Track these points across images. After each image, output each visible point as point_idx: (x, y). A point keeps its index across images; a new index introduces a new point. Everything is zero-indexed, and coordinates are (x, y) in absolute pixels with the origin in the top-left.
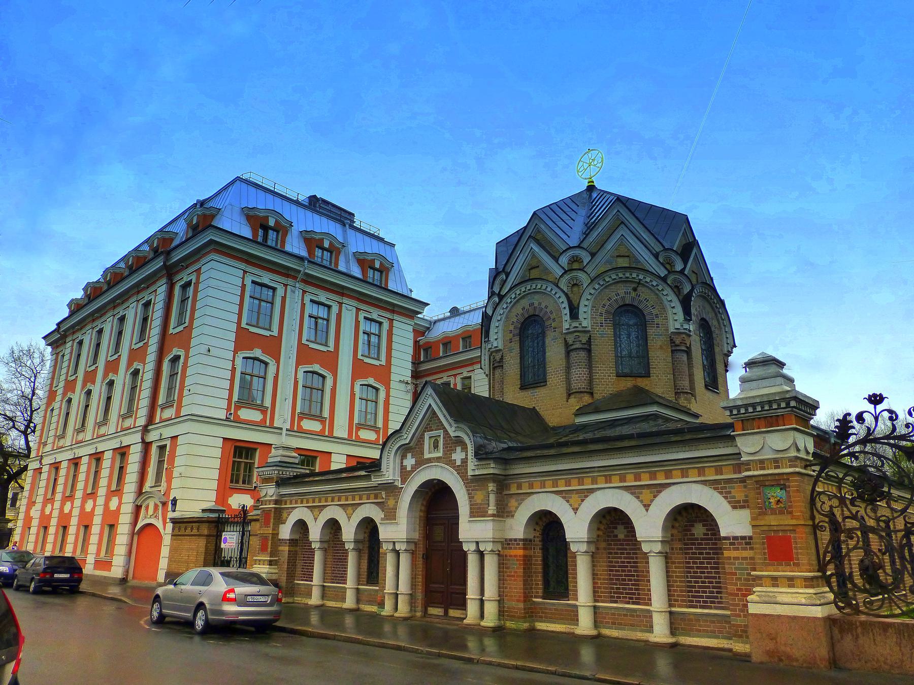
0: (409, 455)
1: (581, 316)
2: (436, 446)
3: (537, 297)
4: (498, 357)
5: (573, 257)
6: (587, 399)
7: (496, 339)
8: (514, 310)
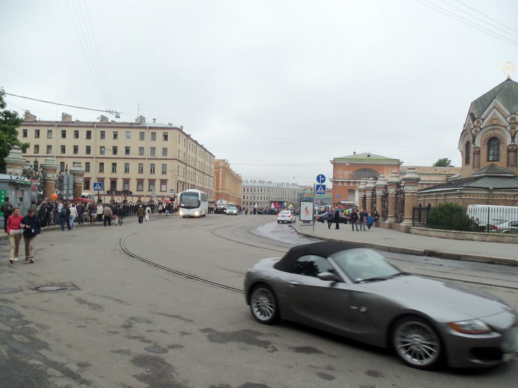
4: (478, 150)
5: (512, 117)
7: (478, 144)
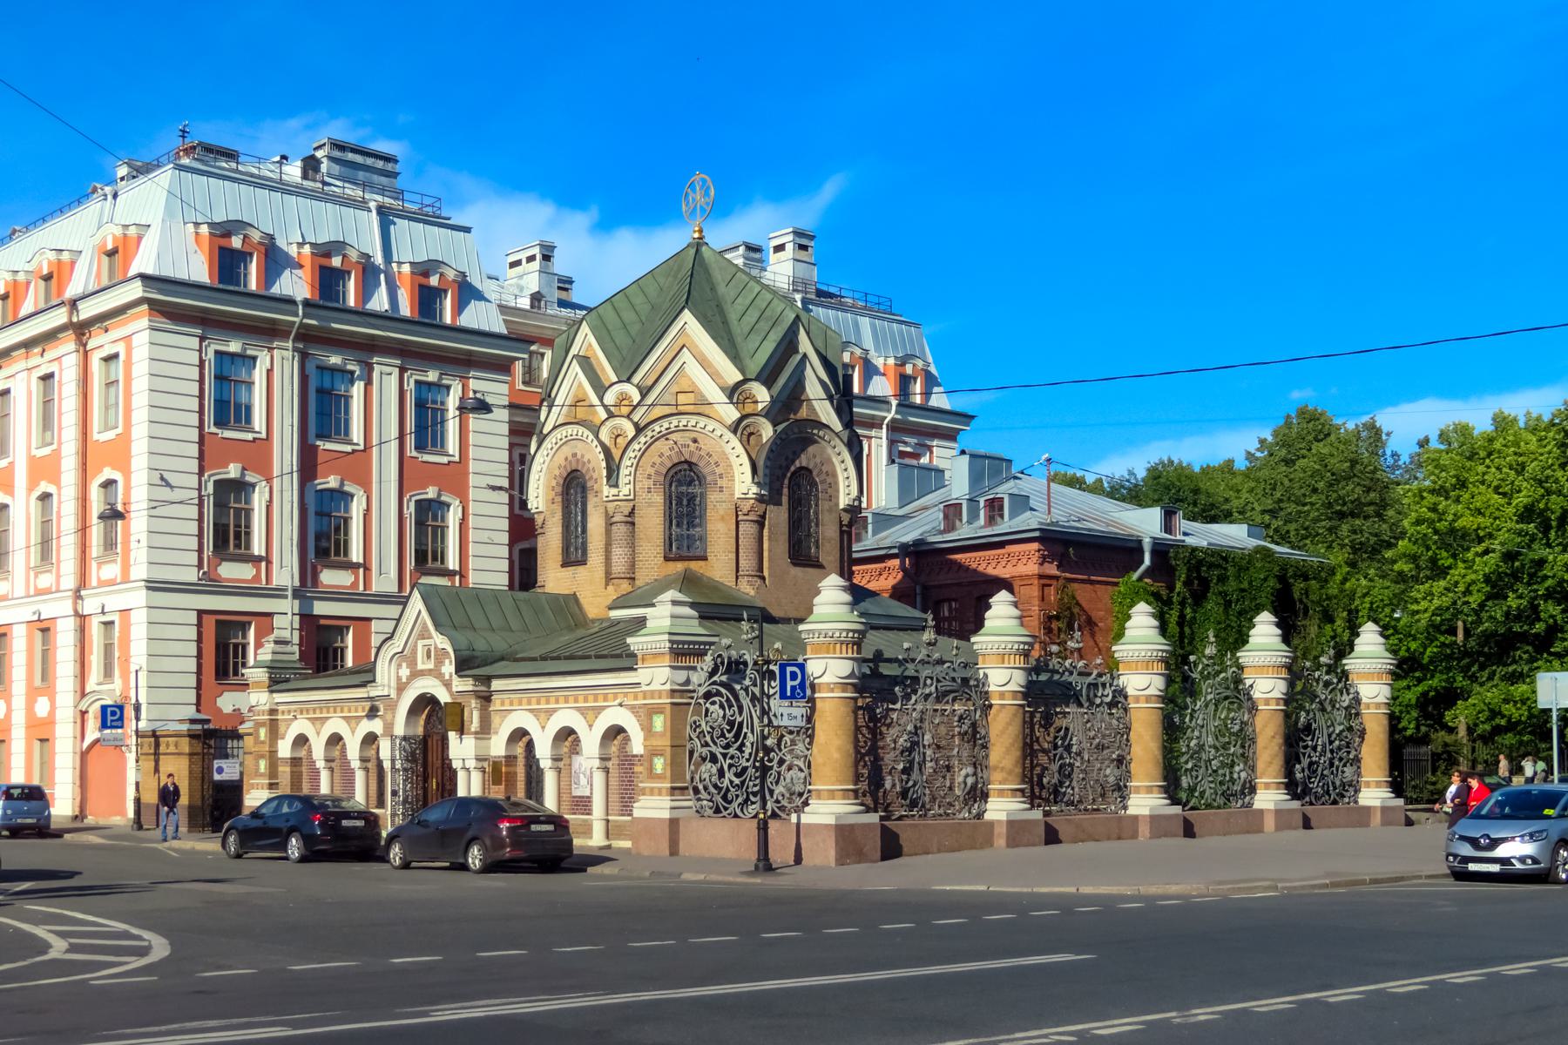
0: (404, 665)
1: (623, 480)
2: (429, 657)
3: (580, 444)
5: (622, 394)
6: (625, 587)
8: (555, 458)
